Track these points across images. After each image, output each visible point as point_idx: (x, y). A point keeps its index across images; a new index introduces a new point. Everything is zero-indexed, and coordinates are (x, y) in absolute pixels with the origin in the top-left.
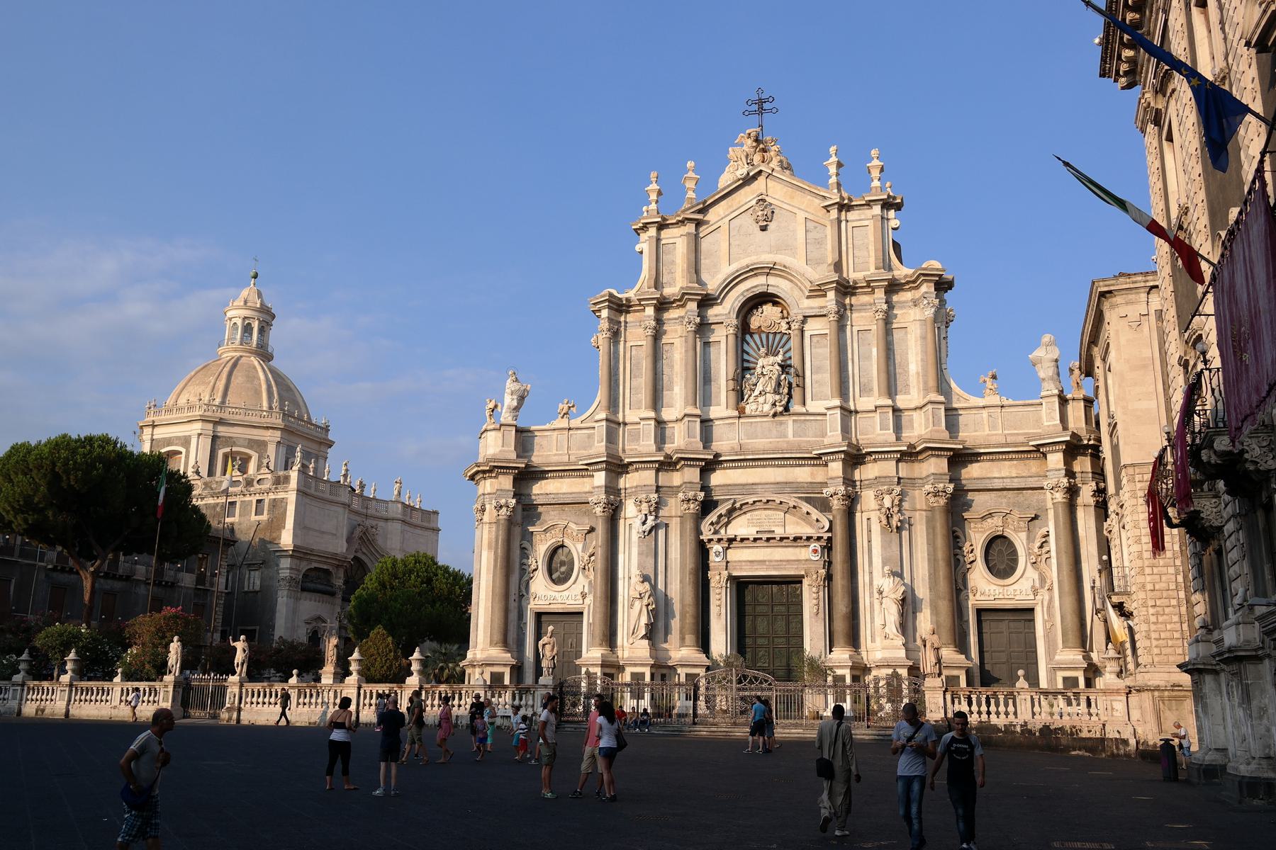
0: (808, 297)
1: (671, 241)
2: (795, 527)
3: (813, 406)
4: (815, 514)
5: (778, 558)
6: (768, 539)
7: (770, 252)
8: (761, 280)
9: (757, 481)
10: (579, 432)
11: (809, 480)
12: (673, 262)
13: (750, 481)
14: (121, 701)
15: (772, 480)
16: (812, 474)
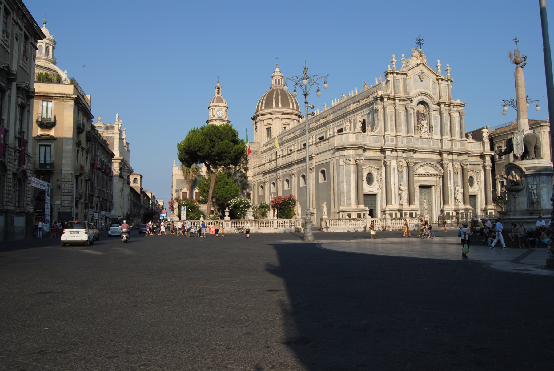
0: (434, 105)
1: (399, 79)
2: (433, 172)
3: (435, 137)
4: (440, 168)
5: (430, 180)
6: (430, 175)
7: (423, 89)
8: (423, 97)
9: (425, 157)
10: (374, 137)
11: (436, 158)
12: (399, 86)
13: (423, 157)
14: (278, 226)
15: (428, 158)
16: (436, 157)
